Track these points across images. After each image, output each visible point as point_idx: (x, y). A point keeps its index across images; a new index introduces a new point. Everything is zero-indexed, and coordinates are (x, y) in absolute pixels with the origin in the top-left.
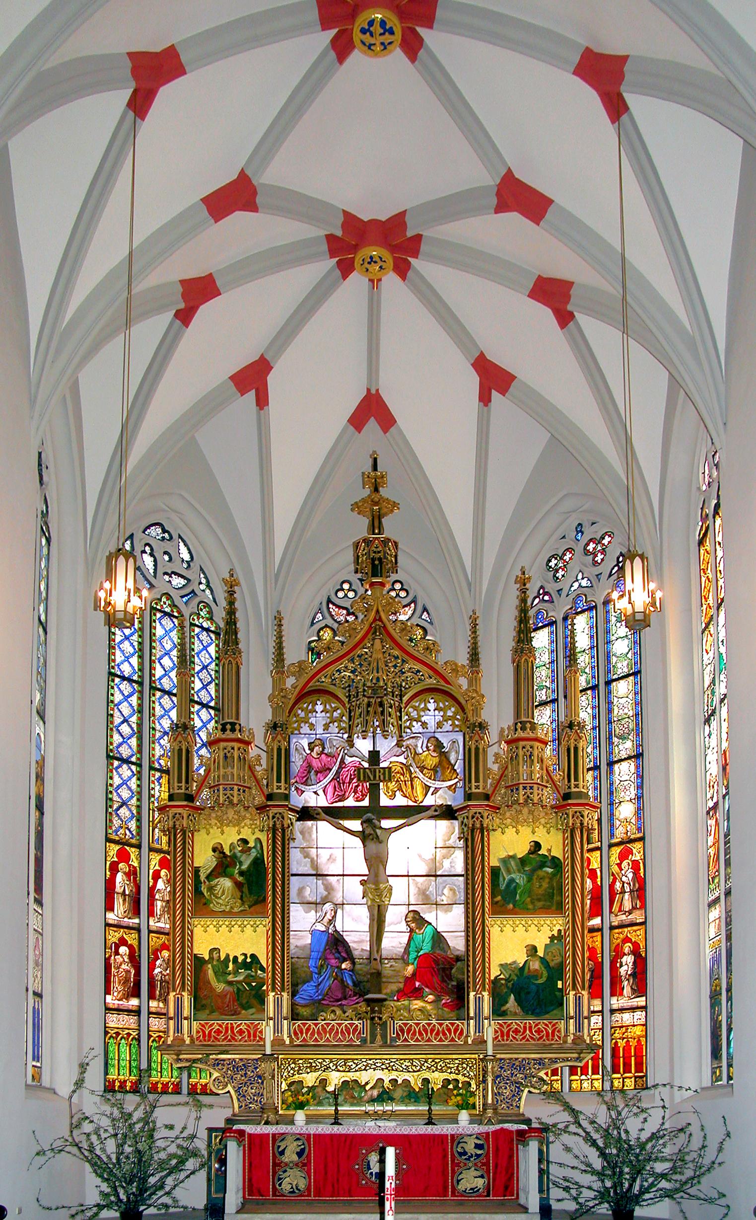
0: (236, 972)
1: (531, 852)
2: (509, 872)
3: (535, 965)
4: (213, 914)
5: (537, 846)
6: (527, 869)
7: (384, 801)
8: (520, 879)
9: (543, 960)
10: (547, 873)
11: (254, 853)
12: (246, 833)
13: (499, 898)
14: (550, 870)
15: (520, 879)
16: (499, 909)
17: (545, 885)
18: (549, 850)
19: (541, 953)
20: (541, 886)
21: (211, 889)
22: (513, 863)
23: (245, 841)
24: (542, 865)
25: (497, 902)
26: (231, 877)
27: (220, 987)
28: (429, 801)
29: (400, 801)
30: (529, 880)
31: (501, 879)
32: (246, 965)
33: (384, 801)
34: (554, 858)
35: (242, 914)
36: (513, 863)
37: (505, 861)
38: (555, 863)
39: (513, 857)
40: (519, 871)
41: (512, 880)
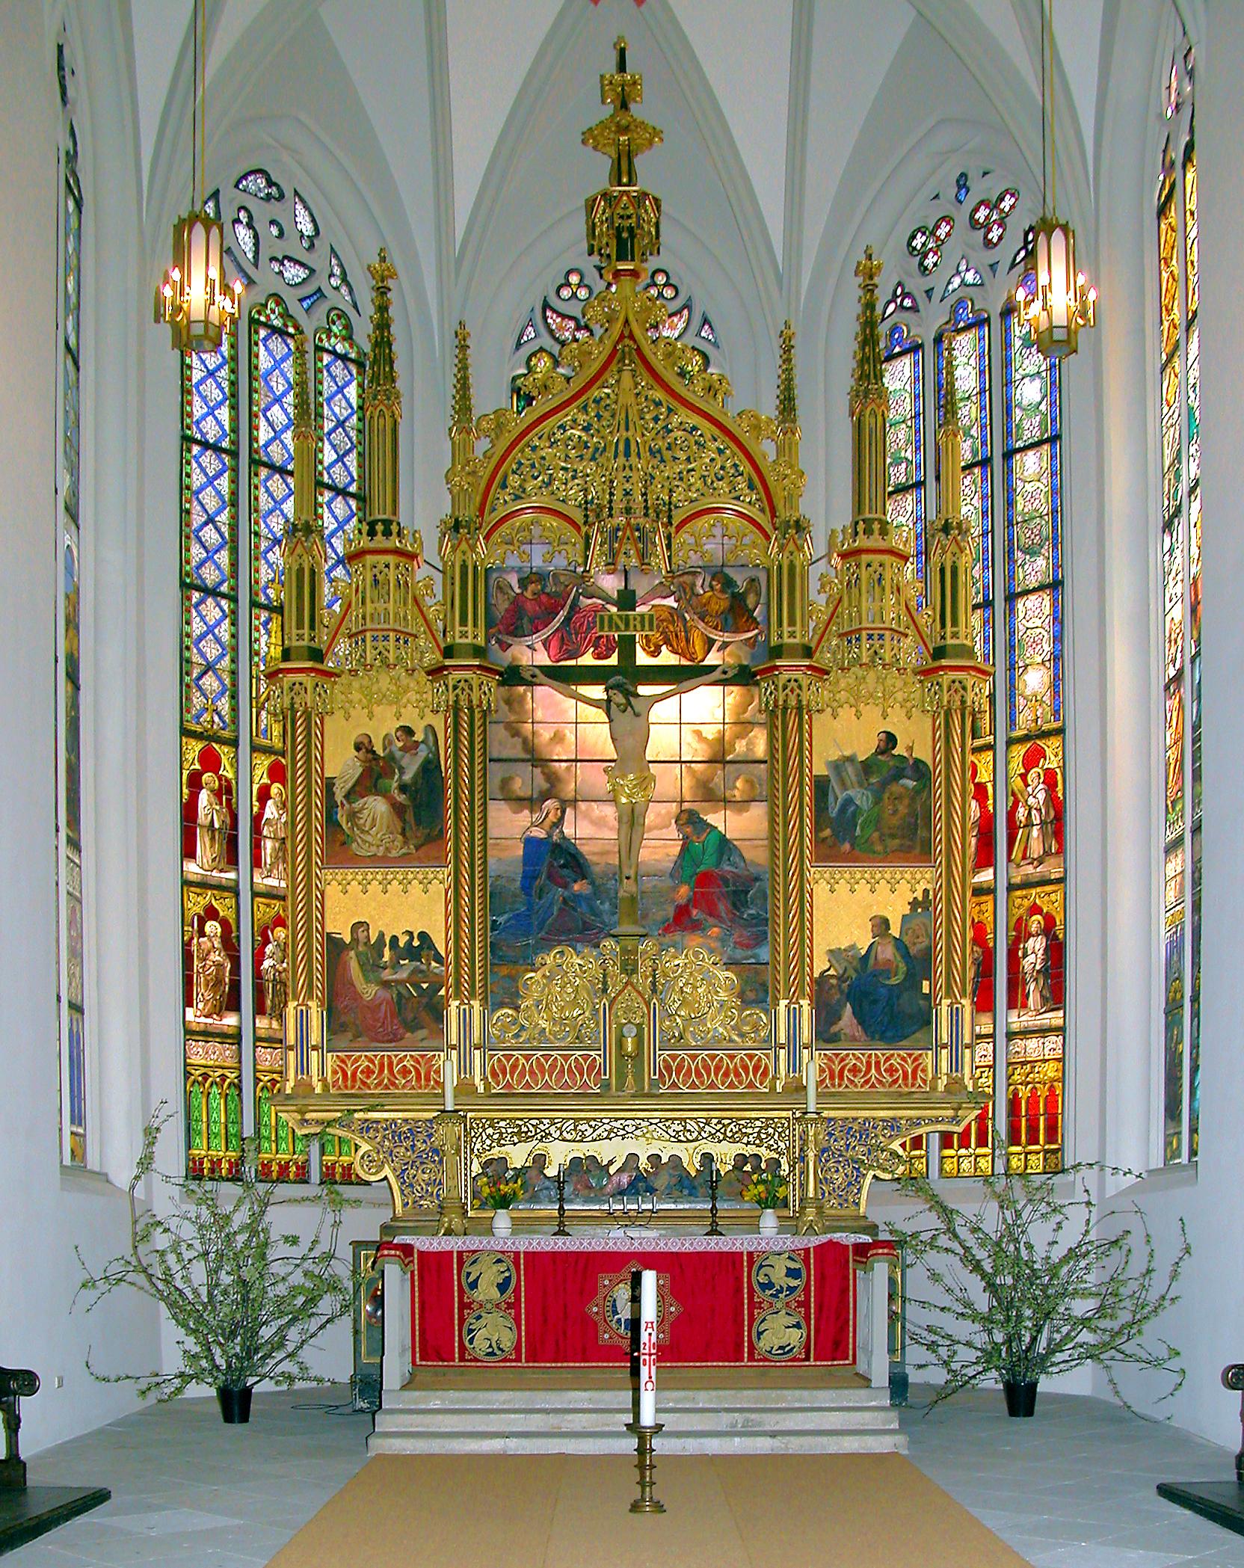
0: (395, 965)
1: (881, 751)
2: (844, 787)
4: (354, 861)
5: (891, 739)
6: (873, 780)
7: (642, 659)
8: (862, 798)
11: (423, 753)
12: (410, 717)
13: (827, 832)
14: (911, 784)
15: (862, 798)
16: (828, 853)
17: (903, 809)
18: (910, 749)
19: (895, 931)
20: (895, 812)
21: (353, 816)
22: (850, 769)
23: (408, 731)
24: (898, 774)
25: (824, 840)
26: (385, 794)
27: (369, 991)
28: (713, 659)
29: (667, 658)
30: (878, 801)
31: (831, 798)
32: (412, 953)
33: (642, 659)
34: (917, 761)
35: (404, 861)
36: (850, 769)
37: (837, 766)
38: (919, 770)
39: (851, 759)
40: (861, 785)
41: (849, 801)
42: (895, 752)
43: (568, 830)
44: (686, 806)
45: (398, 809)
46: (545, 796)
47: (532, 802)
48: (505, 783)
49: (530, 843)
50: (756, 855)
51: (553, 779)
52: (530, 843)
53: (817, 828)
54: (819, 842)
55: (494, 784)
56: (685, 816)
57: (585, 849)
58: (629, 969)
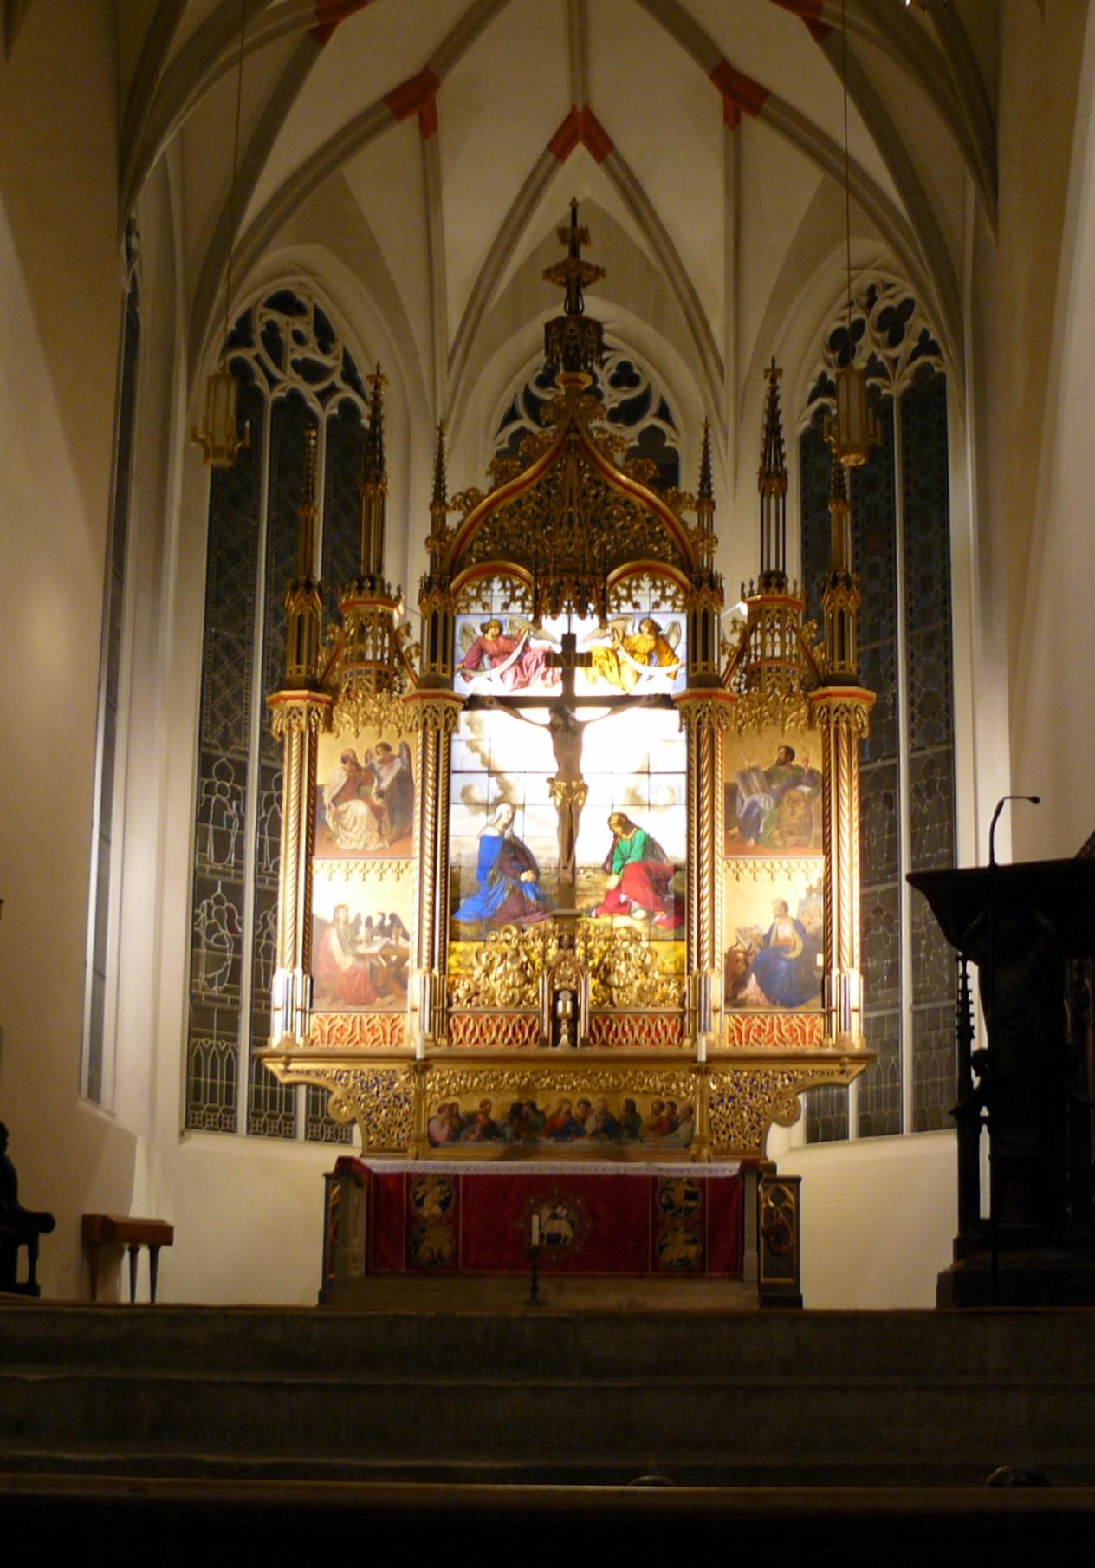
0: (369, 941)
1: (780, 763)
3: (786, 931)
6: (775, 786)
8: (764, 802)
9: (797, 925)
10: (803, 793)
11: (398, 765)
13: (736, 830)
14: (806, 789)
17: (800, 811)
19: (793, 912)
21: (338, 817)
22: (755, 778)
24: (796, 782)
25: (733, 837)
26: (366, 799)
30: (778, 803)
31: (739, 802)
32: (383, 930)
34: (812, 772)
37: (744, 776)
40: (764, 791)
41: (754, 804)
42: (794, 763)
43: (518, 830)
44: (617, 810)
45: (376, 812)
46: (498, 802)
47: (489, 807)
48: (465, 792)
49: (485, 840)
50: (675, 849)
51: (505, 787)
52: (485, 840)
53: (728, 827)
54: (729, 838)
55: (455, 794)
56: (615, 819)
57: (529, 844)
58: (568, 944)
